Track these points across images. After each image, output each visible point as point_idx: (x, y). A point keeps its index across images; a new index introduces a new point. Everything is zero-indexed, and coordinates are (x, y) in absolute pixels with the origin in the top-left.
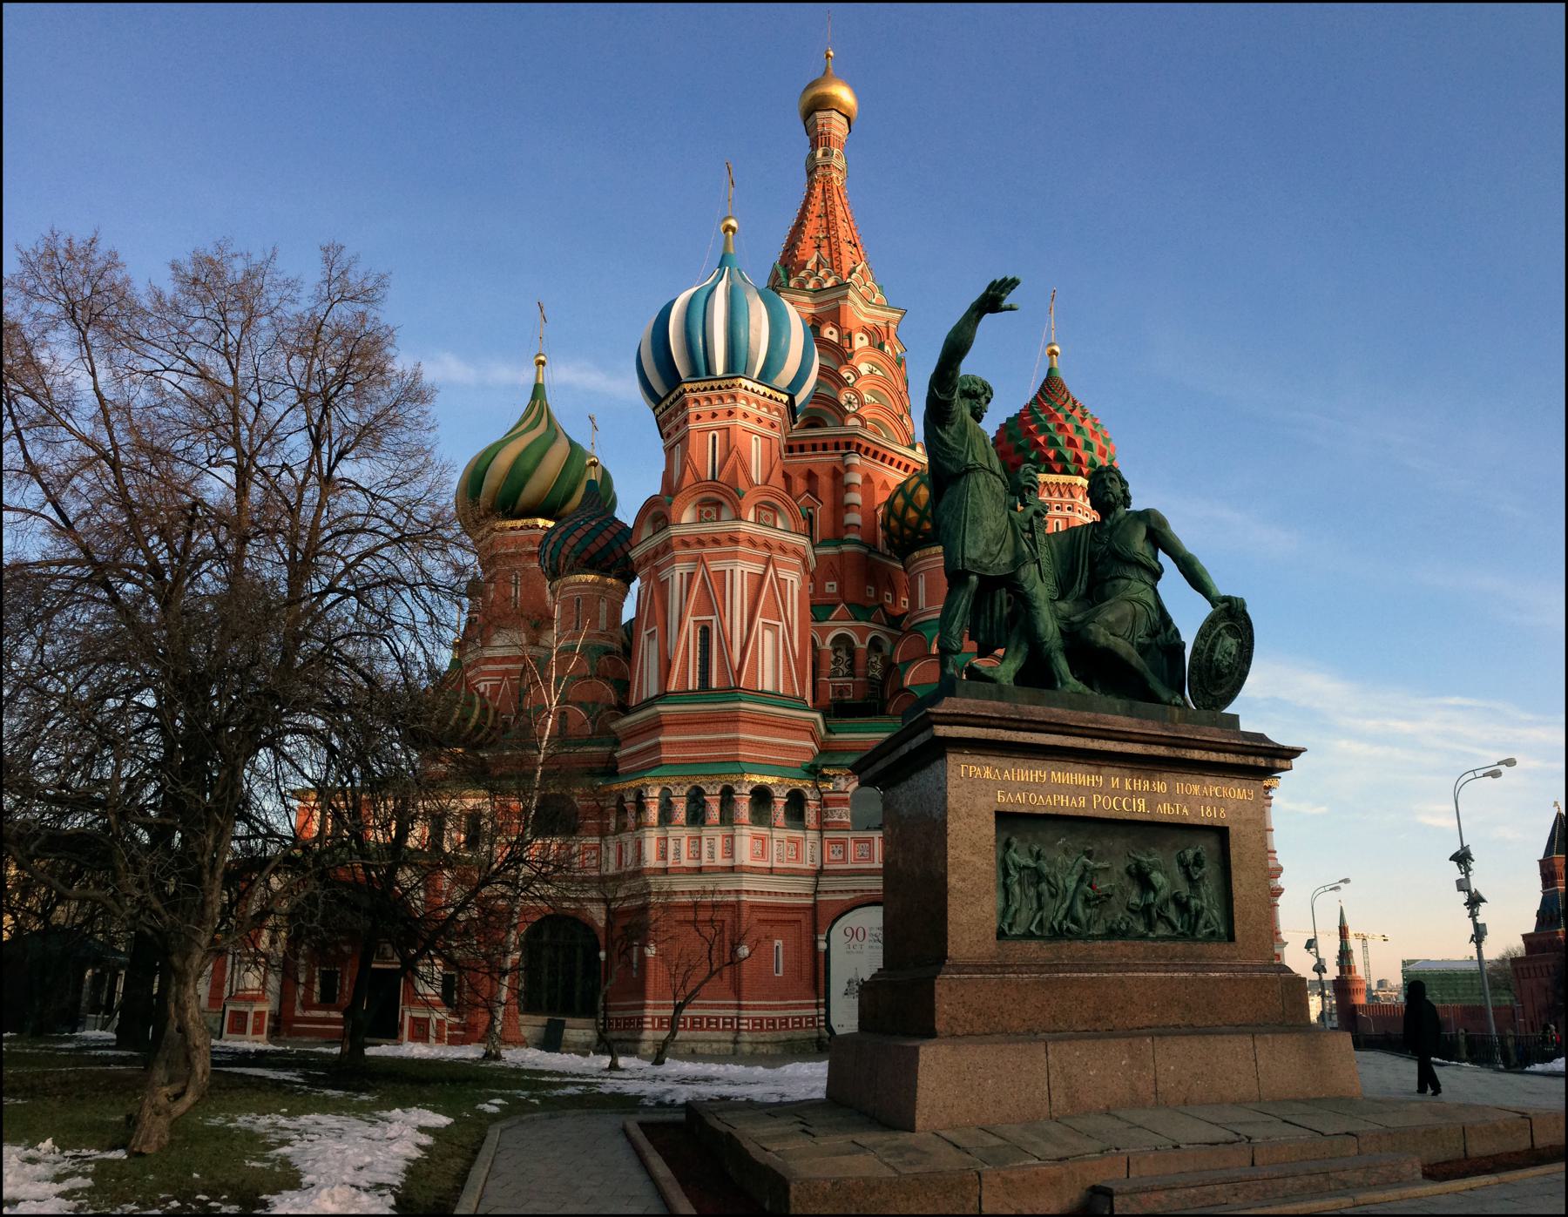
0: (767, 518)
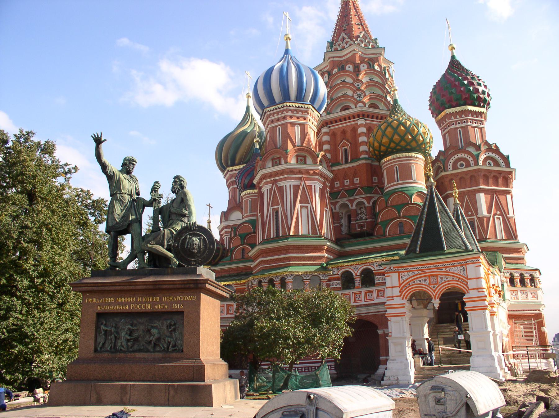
0: (301, 160)
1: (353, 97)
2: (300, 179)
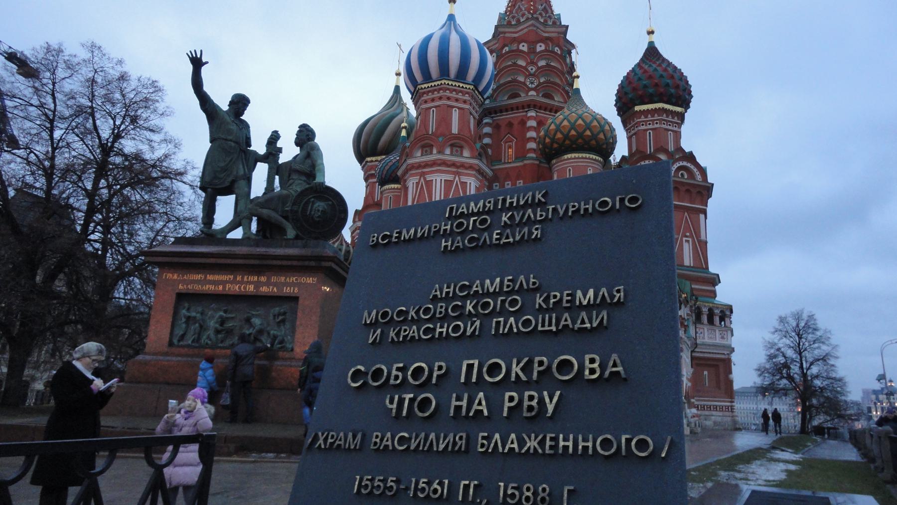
0: (457, 151)
1: (524, 83)
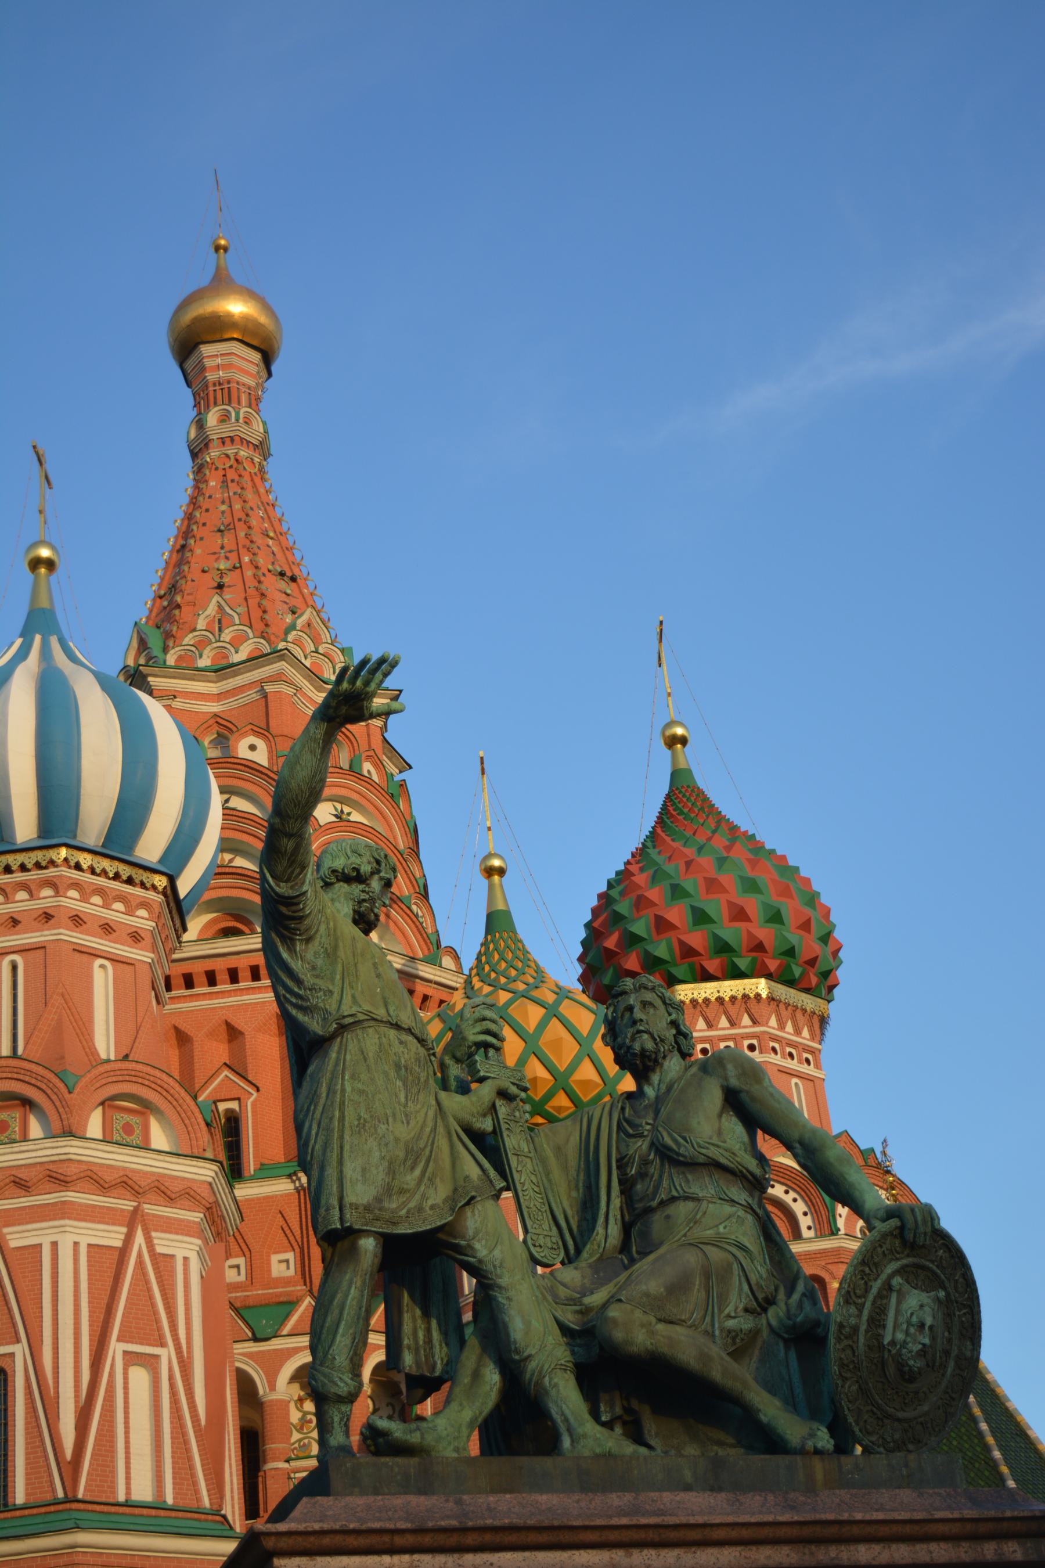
0: (128, 1129)
2: (133, 1220)
